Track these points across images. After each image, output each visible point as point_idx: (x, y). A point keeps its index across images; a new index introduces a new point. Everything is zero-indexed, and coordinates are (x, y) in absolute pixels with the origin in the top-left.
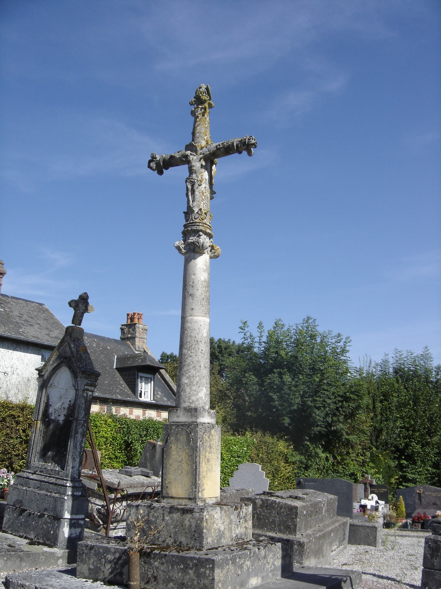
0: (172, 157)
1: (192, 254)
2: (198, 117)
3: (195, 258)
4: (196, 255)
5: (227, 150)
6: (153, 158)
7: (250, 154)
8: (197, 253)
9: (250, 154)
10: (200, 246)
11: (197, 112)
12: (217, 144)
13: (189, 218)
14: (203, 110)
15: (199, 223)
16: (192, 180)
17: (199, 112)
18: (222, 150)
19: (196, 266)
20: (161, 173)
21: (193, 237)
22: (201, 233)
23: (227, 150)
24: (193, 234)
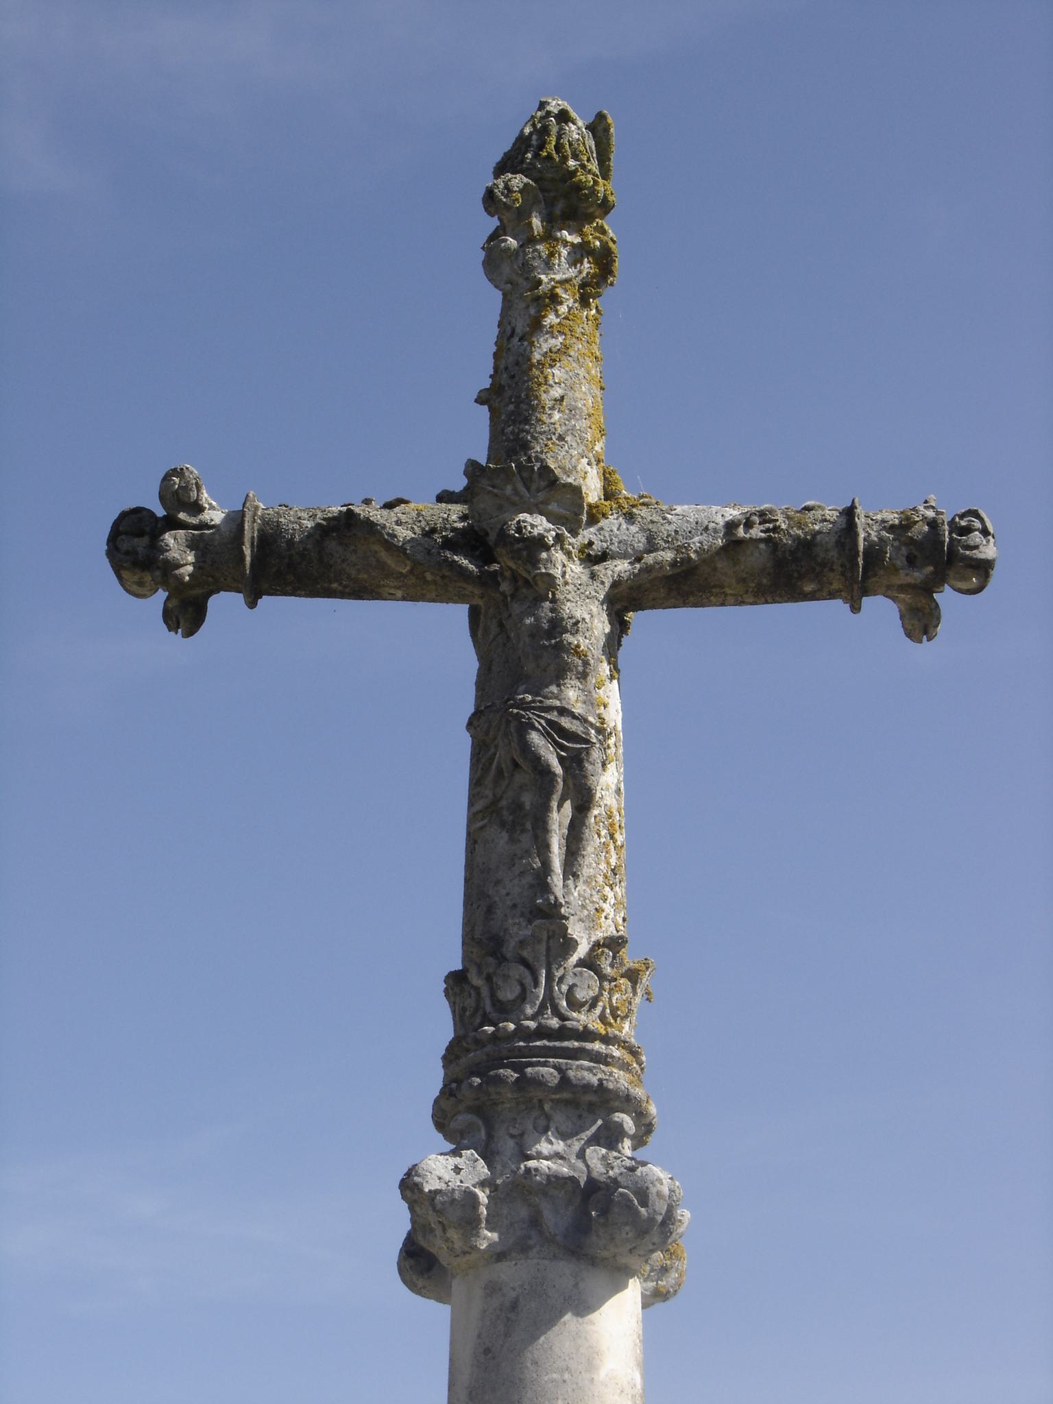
0: (346, 527)
1: (562, 1272)
2: (554, 299)
3: (584, 1306)
4: (594, 1280)
5: (792, 565)
6: (179, 498)
7: (921, 621)
8: (593, 1262)
9: (921, 621)
10: (651, 1220)
11: (549, 266)
12: (733, 513)
13: (523, 997)
14: (587, 266)
15: (606, 1040)
16: (565, 722)
17: (563, 270)
18: (757, 559)
19: (591, 1365)
20: (186, 614)
21: (564, 1136)
22: (628, 1122)
23: (792, 565)
24: (559, 1118)
